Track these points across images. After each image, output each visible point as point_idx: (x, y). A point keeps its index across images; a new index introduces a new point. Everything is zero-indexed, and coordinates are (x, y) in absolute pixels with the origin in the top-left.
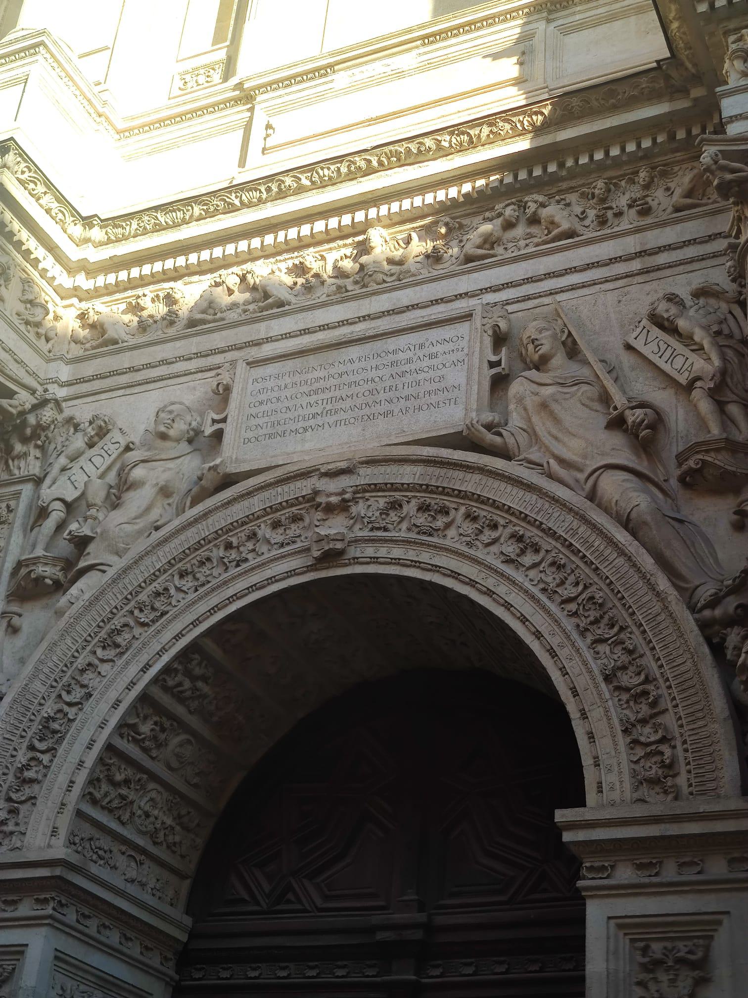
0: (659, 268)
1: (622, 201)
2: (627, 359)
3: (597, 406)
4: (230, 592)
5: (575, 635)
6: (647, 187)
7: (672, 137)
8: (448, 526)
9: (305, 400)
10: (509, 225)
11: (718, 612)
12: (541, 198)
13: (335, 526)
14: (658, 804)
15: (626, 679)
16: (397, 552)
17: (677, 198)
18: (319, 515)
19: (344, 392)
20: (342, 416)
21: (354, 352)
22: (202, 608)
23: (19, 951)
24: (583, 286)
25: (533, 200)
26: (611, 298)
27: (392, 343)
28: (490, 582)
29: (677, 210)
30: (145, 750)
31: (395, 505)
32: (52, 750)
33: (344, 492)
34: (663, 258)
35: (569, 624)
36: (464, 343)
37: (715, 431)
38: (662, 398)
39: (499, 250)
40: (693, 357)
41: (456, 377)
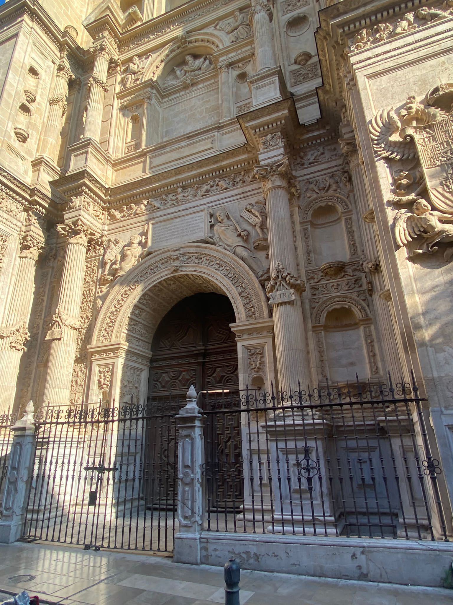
0: (247, 196)
1: (238, 179)
2: (241, 219)
3: (235, 231)
4: (153, 280)
5: (232, 285)
6: (244, 175)
7: (249, 163)
8: (202, 262)
10: (212, 187)
11: (263, 278)
12: (219, 179)
13: (176, 263)
14: (252, 321)
15: (243, 294)
18: (172, 261)
20: (175, 236)
21: (177, 220)
24: (230, 201)
25: (217, 180)
26: (237, 204)
27: (186, 217)
28: (213, 274)
30: (137, 317)
31: (189, 258)
32: (115, 320)
34: (248, 194)
35: (230, 283)
36: (203, 217)
37: (261, 236)
38: (249, 228)
39: (210, 193)
40: (256, 218)
41: (202, 225)
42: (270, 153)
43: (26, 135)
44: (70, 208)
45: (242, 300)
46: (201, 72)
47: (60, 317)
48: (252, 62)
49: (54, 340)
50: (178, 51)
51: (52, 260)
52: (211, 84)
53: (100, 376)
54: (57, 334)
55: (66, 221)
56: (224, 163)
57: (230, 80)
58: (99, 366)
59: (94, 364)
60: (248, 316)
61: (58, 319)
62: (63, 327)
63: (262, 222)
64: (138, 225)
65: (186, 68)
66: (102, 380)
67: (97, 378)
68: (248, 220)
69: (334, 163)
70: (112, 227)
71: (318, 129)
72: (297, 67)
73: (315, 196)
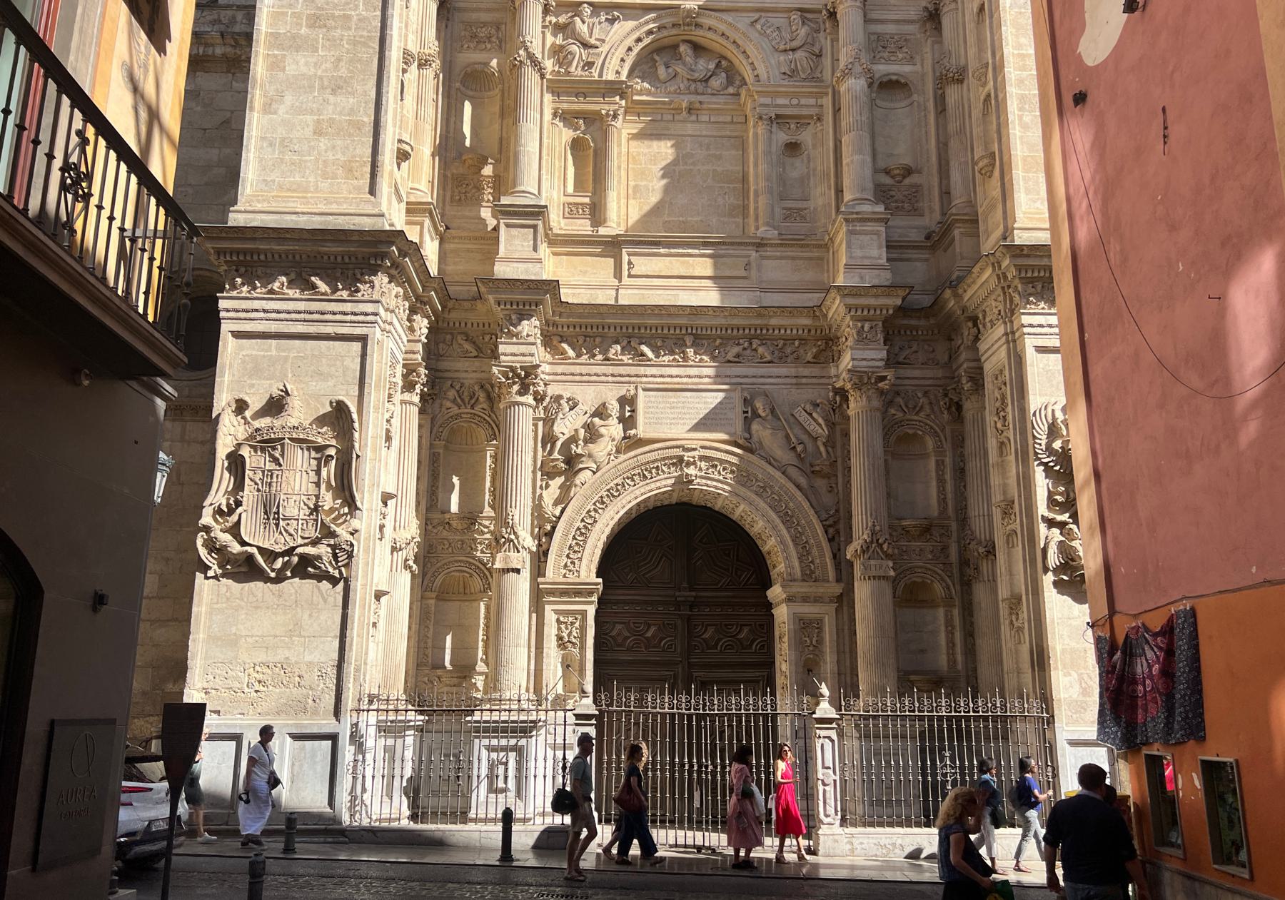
2: (792, 420)
7: (809, 331)
9: (669, 411)
11: (827, 523)
16: (715, 483)
17: (809, 357)
19: (686, 410)
22: (638, 492)
23: (584, 613)
25: (755, 343)
27: (704, 394)
29: (809, 362)
32: (585, 542)
33: (694, 457)
34: (804, 381)
37: (824, 454)
38: (804, 437)
40: (818, 427)
42: (868, 352)
43: (410, 151)
44: (510, 334)
45: (796, 548)
46: (709, 91)
47: (515, 533)
48: (811, 129)
49: (508, 570)
50: (674, 32)
51: (430, 401)
52: (725, 123)
53: (559, 629)
54: (515, 561)
55: (503, 358)
56: (774, 322)
57: (774, 149)
58: (556, 611)
59: (548, 608)
60: (802, 575)
61: (512, 537)
62: (520, 548)
63: (829, 436)
64: (610, 379)
65: (679, 69)
66: (565, 635)
67: (554, 631)
68: (805, 425)
69: (929, 373)
70: (560, 369)
71: (919, 318)
72: (887, 180)
73: (900, 414)
